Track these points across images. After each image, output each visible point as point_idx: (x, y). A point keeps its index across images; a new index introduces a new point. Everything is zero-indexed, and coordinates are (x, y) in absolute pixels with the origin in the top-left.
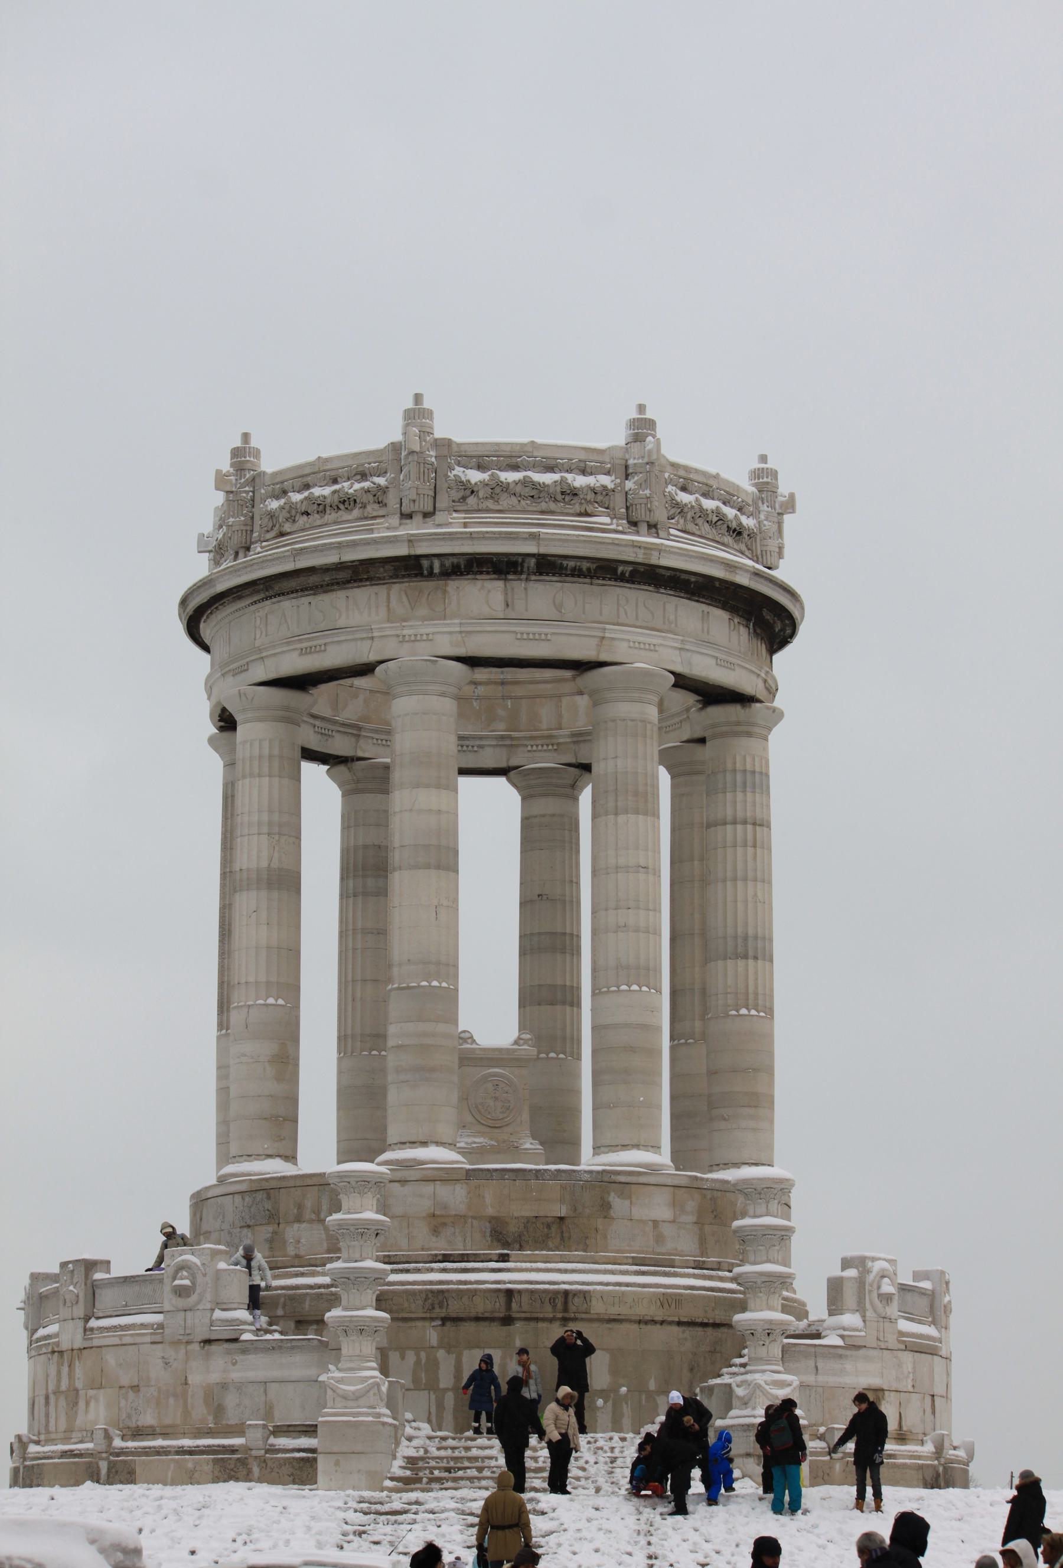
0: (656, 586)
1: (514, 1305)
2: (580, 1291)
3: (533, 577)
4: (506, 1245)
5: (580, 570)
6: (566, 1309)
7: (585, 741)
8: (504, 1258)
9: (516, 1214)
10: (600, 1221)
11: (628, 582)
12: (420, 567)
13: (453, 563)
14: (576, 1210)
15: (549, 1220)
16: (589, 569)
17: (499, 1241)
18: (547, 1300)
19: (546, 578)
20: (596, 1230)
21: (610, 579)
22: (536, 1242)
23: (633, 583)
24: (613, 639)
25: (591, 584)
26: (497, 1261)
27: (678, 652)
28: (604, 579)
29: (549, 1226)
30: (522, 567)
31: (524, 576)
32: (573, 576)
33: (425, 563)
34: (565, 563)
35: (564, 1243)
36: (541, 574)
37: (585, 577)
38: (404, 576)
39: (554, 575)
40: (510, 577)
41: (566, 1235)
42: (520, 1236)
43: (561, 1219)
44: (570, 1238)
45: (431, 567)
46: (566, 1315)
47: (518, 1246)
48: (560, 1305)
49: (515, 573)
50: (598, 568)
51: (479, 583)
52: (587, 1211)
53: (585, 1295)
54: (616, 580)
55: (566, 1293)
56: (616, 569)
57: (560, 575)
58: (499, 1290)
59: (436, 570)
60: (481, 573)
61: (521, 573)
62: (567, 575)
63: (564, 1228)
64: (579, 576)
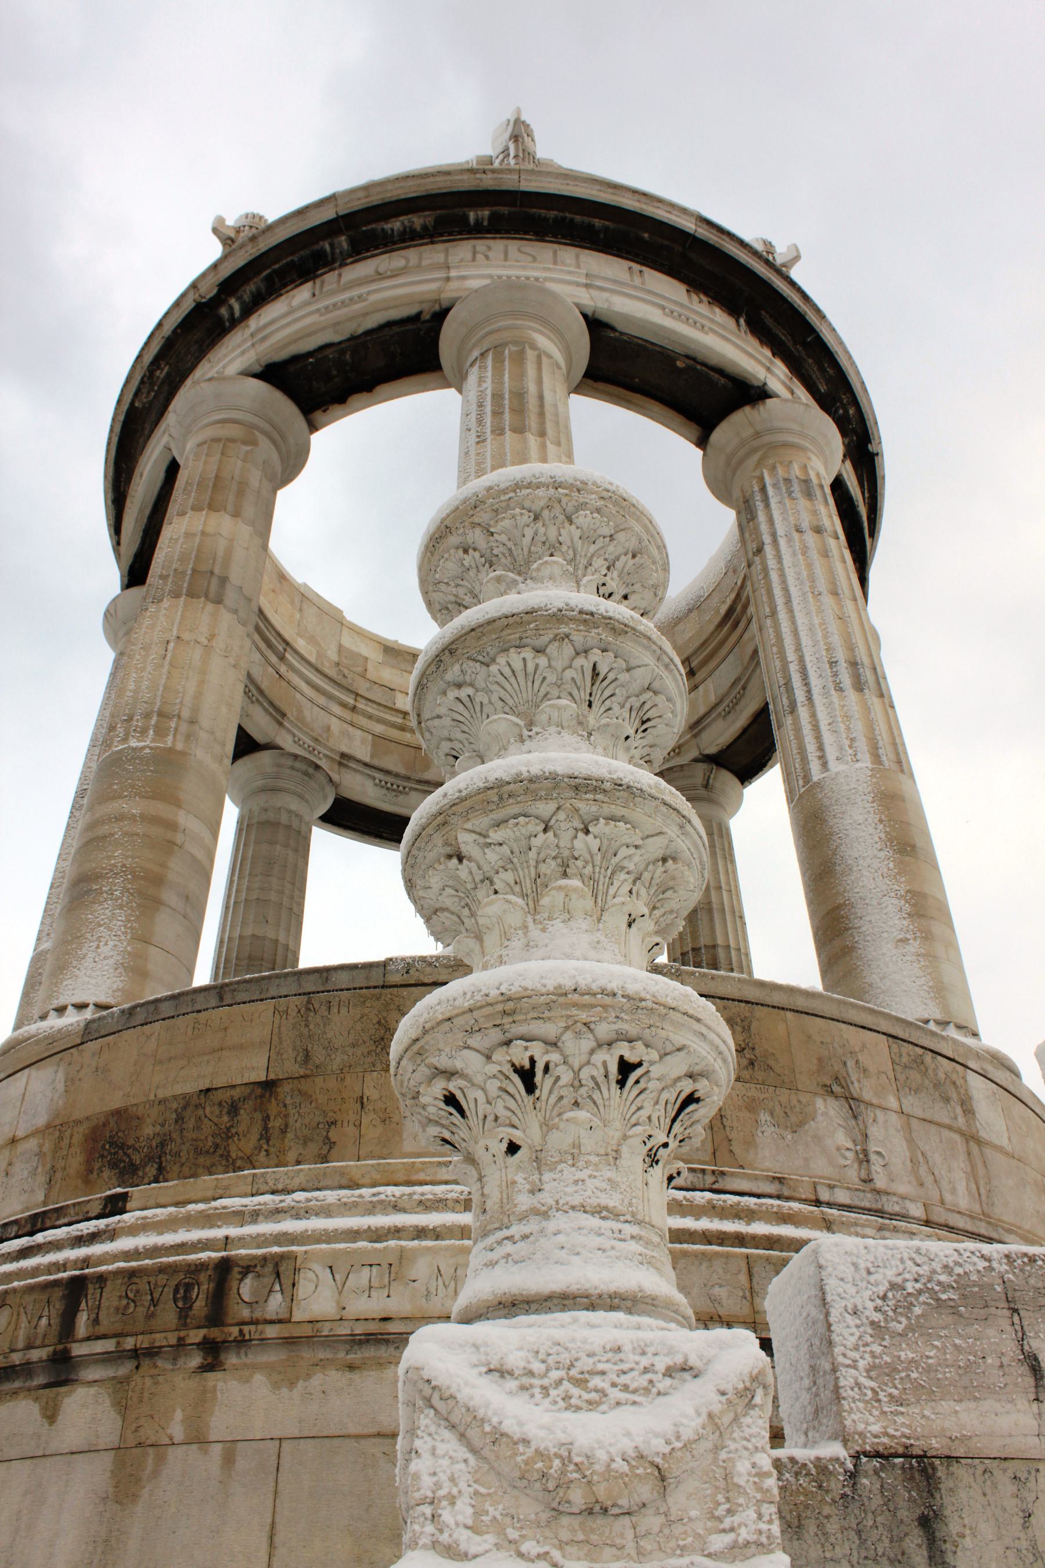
0: (536, 234)
1: (82, 1320)
2: (265, 1259)
3: (351, 260)
4: (129, 1173)
5: (413, 231)
6: (216, 1316)
7: (704, 728)
8: (116, 1205)
9: (161, 1094)
10: (371, 1078)
11: (489, 232)
12: (220, 319)
13: (252, 293)
14: (307, 1056)
15: (236, 1093)
16: (425, 227)
17: (113, 1165)
18: (169, 1293)
19: (369, 254)
20: (361, 1101)
21: (460, 233)
22: (198, 1152)
23: (498, 232)
24: (464, 278)
25: (432, 243)
26: (97, 1218)
27: (584, 290)
28: (450, 234)
29: (234, 1109)
30: (333, 253)
31: (337, 264)
32: (404, 241)
33: (223, 311)
34: (387, 226)
35: (270, 1145)
36: (359, 253)
37: (422, 237)
38: (208, 347)
39: (377, 248)
40: (320, 272)
41: (276, 1123)
42: (162, 1145)
43: (269, 1086)
44: (284, 1131)
45: (232, 314)
46: (215, 1333)
47: (151, 1170)
48: (200, 1306)
49: (325, 266)
50: (438, 221)
51: (283, 298)
52: (339, 1059)
53: (279, 1269)
54: (469, 232)
55: (224, 1267)
56: (466, 218)
57: (385, 245)
58: (56, 1283)
59: (237, 314)
60: (285, 286)
61: (334, 261)
62: (394, 243)
63: (273, 1108)
64: (413, 239)
